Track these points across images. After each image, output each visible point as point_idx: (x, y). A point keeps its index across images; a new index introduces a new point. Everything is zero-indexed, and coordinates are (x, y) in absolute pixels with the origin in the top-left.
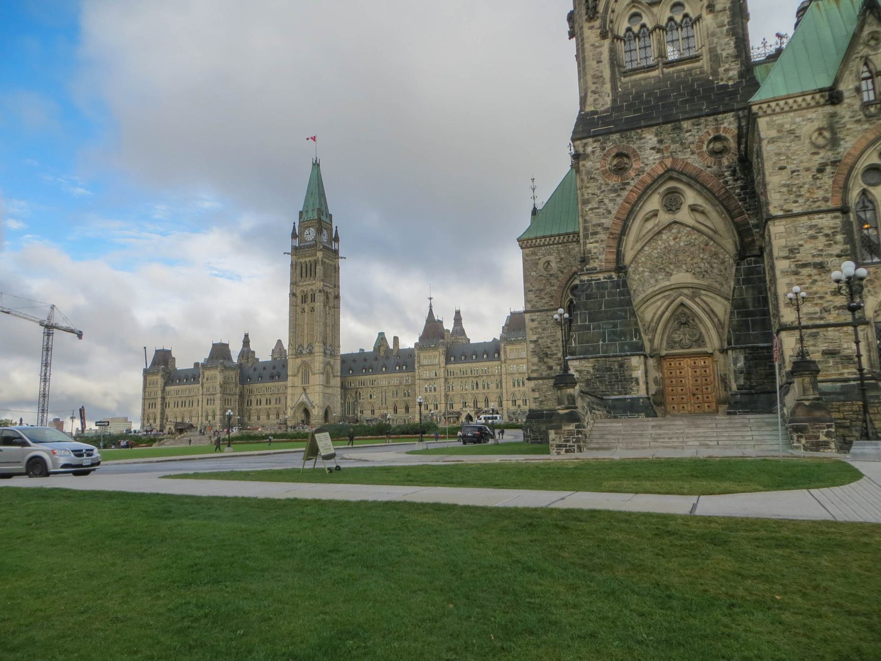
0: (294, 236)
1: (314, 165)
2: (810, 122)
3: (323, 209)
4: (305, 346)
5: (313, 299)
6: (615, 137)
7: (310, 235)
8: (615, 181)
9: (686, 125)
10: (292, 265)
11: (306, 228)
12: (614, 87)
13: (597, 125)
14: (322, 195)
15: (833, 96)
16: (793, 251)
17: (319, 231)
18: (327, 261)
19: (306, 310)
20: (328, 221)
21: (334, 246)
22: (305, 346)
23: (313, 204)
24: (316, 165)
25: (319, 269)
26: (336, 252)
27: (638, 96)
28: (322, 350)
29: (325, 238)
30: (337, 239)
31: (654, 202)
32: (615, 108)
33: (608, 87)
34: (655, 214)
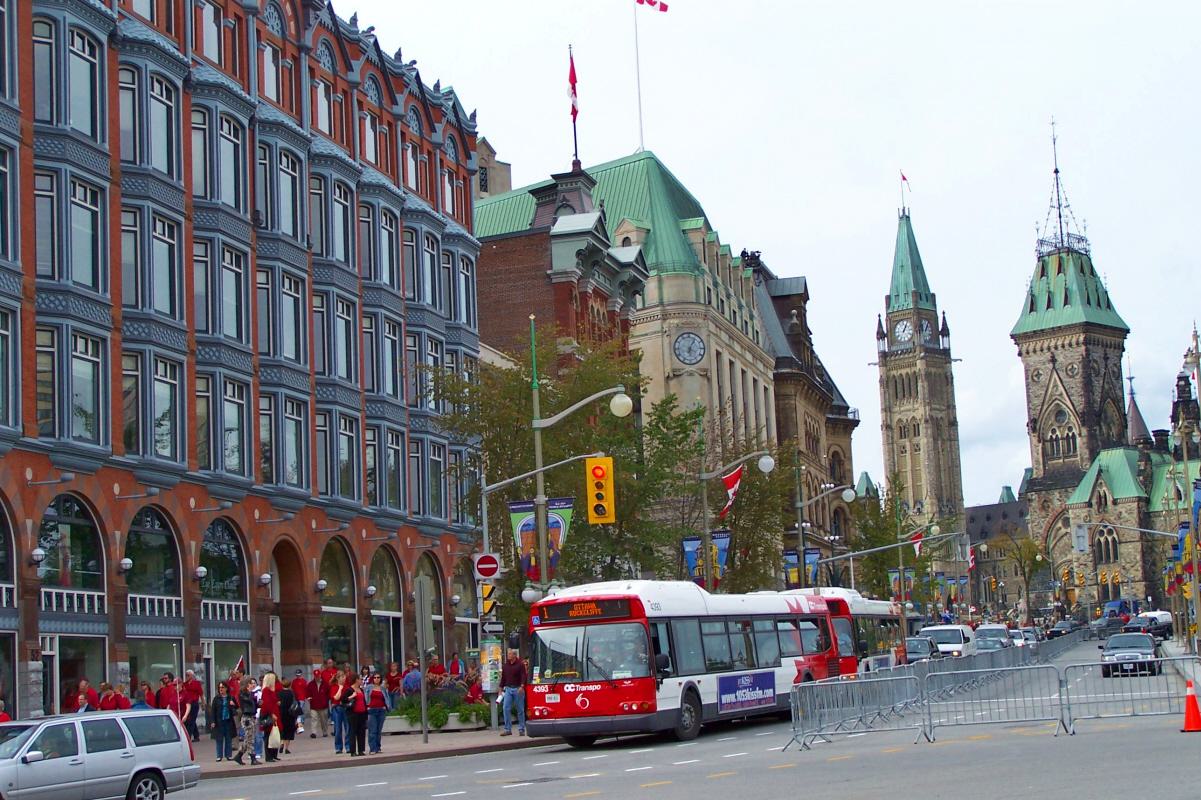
0: (881, 335)
1: (901, 218)
2: (1084, 512)
3: (922, 290)
4: (911, 504)
5: (917, 433)
6: (1044, 492)
7: (904, 332)
8: (1044, 513)
9: (1070, 490)
10: (881, 381)
11: (898, 322)
12: (1044, 467)
13: (1036, 486)
14: (917, 266)
15: (1089, 504)
16: (1078, 559)
17: (919, 329)
18: (933, 370)
19: (908, 448)
20: (928, 306)
21: (943, 343)
22: (911, 504)
23: (906, 285)
24: (905, 218)
25: (922, 386)
26: (947, 352)
27: (1053, 473)
28: (935, 509)
29: (927, 334)
30: (945, 332)
31: (1060, 524)
32: (1044, 478)
33: (1041, 466)
34: (1060, 528)
